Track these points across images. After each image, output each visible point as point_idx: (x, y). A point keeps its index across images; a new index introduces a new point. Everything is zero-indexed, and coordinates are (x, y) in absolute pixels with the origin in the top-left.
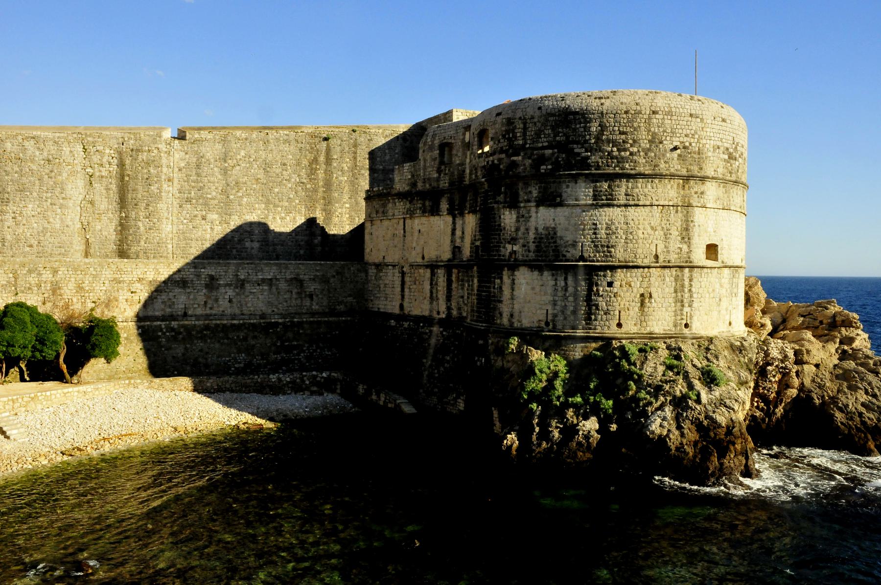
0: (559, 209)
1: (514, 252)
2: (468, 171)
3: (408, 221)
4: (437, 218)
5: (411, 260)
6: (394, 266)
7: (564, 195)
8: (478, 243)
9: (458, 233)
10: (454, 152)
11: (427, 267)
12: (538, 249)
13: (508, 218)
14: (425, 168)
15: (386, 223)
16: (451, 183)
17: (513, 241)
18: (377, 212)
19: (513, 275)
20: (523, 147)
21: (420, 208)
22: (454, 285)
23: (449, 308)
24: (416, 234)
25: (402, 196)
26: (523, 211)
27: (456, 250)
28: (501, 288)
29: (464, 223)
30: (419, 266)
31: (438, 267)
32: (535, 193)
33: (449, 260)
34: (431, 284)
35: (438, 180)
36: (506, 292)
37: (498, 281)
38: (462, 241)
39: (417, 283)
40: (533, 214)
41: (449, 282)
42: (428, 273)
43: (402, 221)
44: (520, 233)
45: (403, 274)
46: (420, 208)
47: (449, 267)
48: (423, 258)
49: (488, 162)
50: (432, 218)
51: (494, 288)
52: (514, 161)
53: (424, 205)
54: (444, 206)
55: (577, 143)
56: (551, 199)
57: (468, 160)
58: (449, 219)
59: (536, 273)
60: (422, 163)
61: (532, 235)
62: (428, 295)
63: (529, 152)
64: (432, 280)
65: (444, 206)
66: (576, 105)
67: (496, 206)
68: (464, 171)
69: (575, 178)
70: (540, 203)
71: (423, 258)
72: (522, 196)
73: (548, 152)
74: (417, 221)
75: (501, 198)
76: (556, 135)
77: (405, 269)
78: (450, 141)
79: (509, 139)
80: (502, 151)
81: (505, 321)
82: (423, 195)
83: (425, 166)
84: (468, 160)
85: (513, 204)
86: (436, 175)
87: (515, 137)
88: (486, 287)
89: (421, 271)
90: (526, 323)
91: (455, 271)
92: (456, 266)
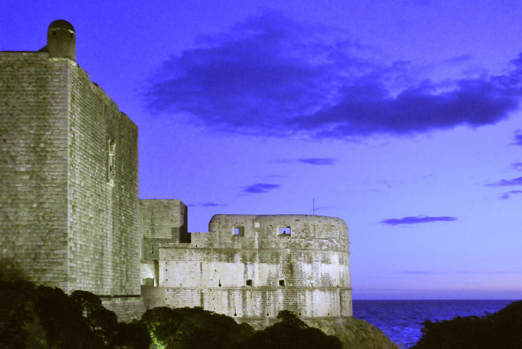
0: (329, 265)
1: (312, 284)
2: (256, 242)
4: (230, 264)
5: (209, 286)
6: (192, 290)
7: (331, 260)
8: (283, 279)
9: (250, 273)
10: (245, 231)
11: (224, 290)
12: (323, 282)
13: (306, 268)
14: (220, 237)
15: (182, 264)
16: (244, 248)
17: (311, 278)
18: (173, 257)
19: (312, 294)
20: (314, 237)
21: (217, 258)
22: (248, 300)
23: (244, 312)
26: (314, 265)
27: (249, 283)
28: (305, 300)
29: (254, 267)
30: (217, 290)
31: (234, 290)
32: (320, 258)
33: (243, 287)
34: (229, 299)
35: (232, 244)
37: (302, 297)
38: (253, 277)
39: (216, 299)
40: (320, 267)
41: (244, 299)
42: (226, 294)
44: (314, 275)
45: (202, 294)
46: (217, 258)
47: (243, 291)
48: (220, 285)
49: (290, 241)
50: (227, 264)
51: (300, 300)
52: (309, 243)
53: (220, 257)
55: (334, 238)
56: (326, 261)
57: (257, 237)
58: (243, 265)
59: (323, 292)
61: (320, 276)
62: (227, 305)
63: (317, 240)
64: (228, 297)
65: (238, 257)
67: (298, 262)
68: (254, 242)
70: (323, 262)
71: (220, 285)
72: (314, 258)
73: (325, 241)
75: (302, 258)
76: (327, 234)
77: (204, 292)
78: (242, 225)
79: (306, 233)
80: (301, 237)
82: (219, 251)
85: (310, 262)
86: (230, 242)
87: (310, 232)
88: (293, 299)
89: (219, 292)
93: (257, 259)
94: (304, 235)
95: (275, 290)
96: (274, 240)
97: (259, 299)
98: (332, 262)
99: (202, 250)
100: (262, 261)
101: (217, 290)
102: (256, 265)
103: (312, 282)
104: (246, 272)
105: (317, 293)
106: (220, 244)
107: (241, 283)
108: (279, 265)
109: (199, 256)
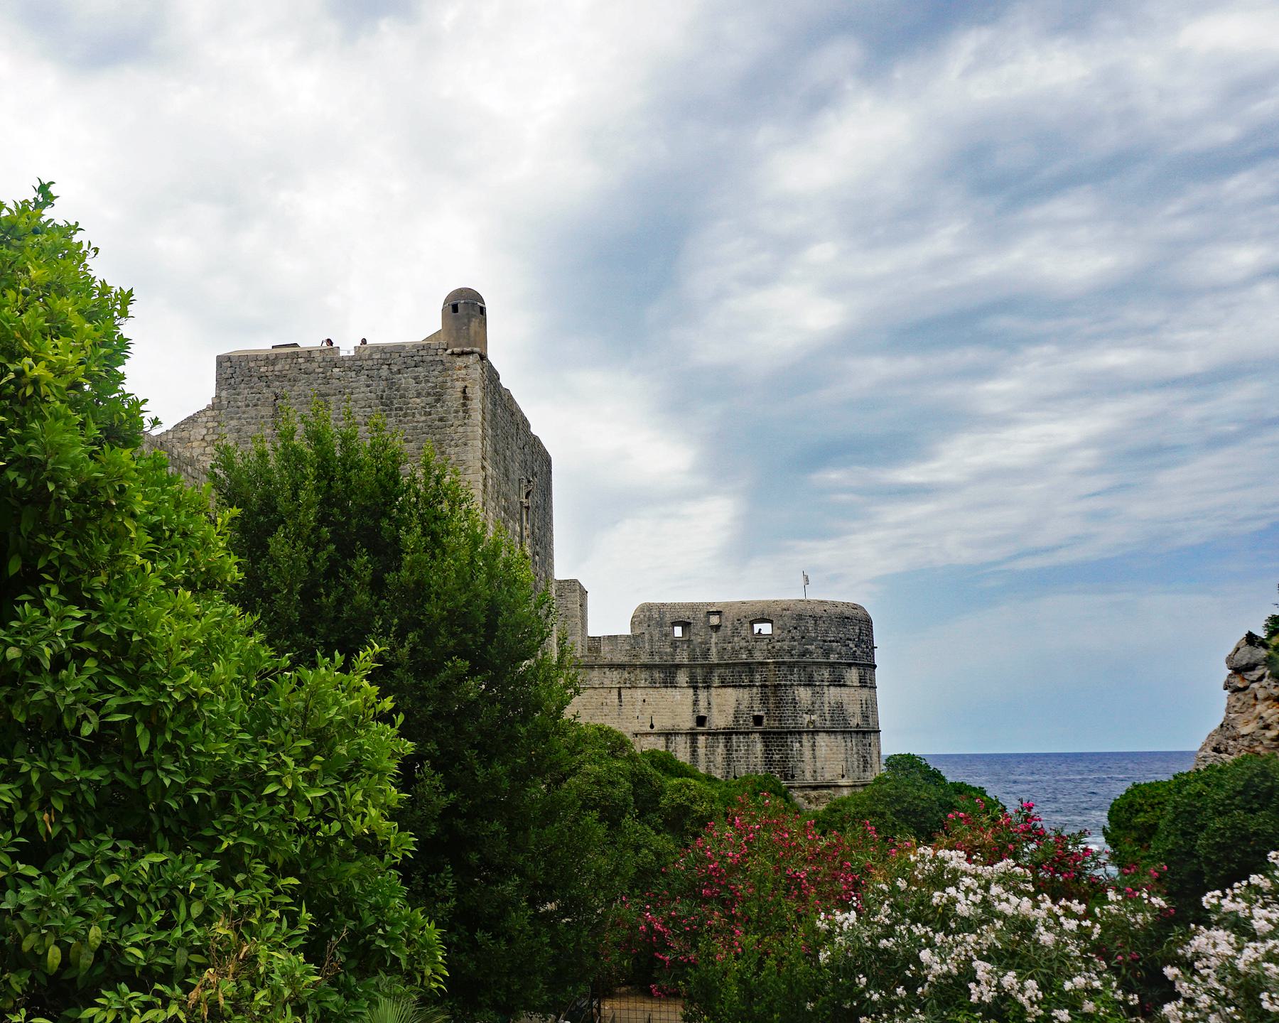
1: (813, 722)
3: (623, 692)
8: (761, 713)
9: (703, 703)
11: (659, 734)
20: (815, 639)
22: (701, 751)
24: (641, 703)
25: (612, 666)
27: (701, 721)
30: (647, 734)
31: (676, 734)
32: (826, 675)
35: (673, 655)
36: (807, 753)
43: (615, 692)
47: (693, 735)
48: (652, 726)
54: (682, 678)
56: (838, 682)
58: (691, 691)
60: (647, 636)
65: (682, 678)
66: (847, 614)
69: (850, 665)
71: (652, 726)
72: (816, 677)
74: (639, 691)
81: (808, 775)
82: (646, 667)
83: (651, 640)
84: (713, 640)
85: (809, 684)
89: (652, 739)
90: (828, 776)
91: (701, 739)
92: (703, 734)
93: (716, 682)
94: (797, 634)
95: (747, 733)
96: (743, 644)
97: (721, 749)
98: (849, 683)
99: (621, 667)
100: (724, 685)
101: (647, 734)
102: (713, 691)
103: (813, 717)
104: (696, 703)
105: (822, 740)
106: (652, 654)
107: (688, 723)
108: (755, 690)
109: (614, 677)
